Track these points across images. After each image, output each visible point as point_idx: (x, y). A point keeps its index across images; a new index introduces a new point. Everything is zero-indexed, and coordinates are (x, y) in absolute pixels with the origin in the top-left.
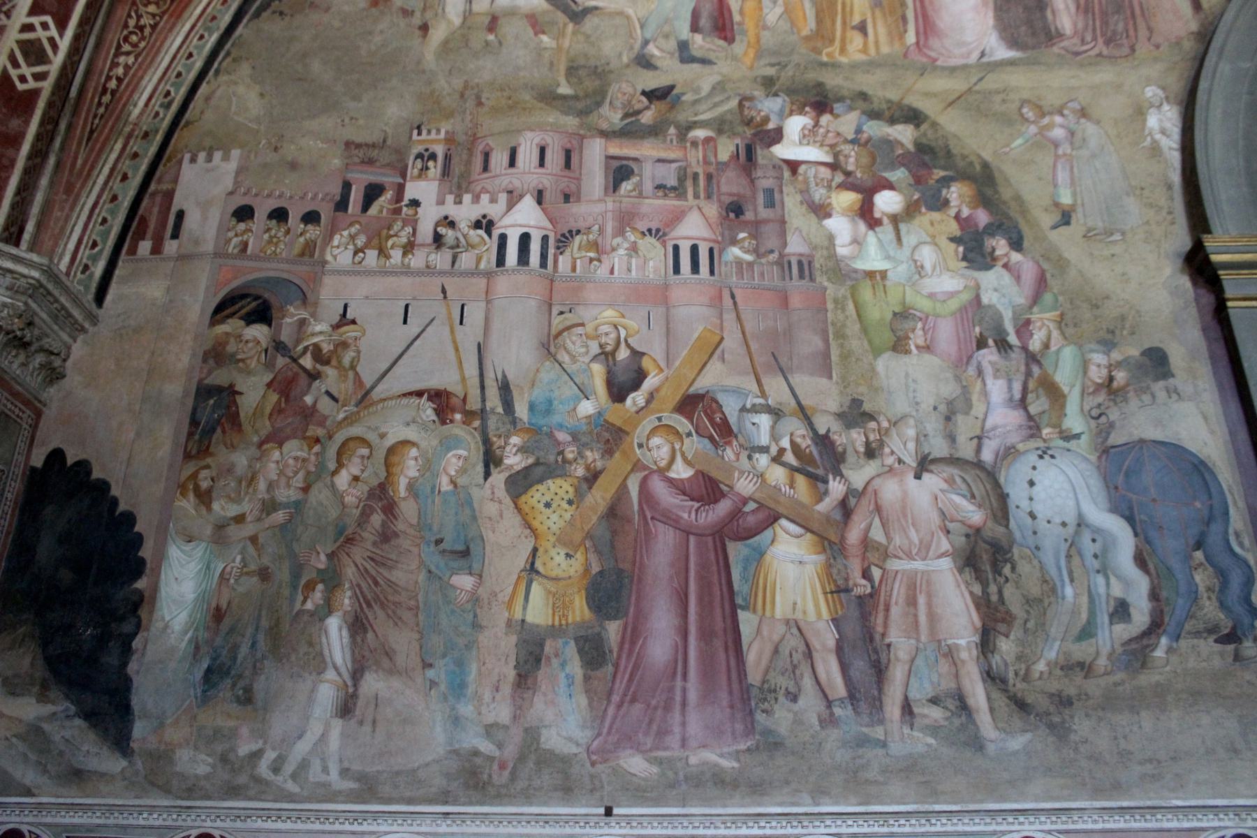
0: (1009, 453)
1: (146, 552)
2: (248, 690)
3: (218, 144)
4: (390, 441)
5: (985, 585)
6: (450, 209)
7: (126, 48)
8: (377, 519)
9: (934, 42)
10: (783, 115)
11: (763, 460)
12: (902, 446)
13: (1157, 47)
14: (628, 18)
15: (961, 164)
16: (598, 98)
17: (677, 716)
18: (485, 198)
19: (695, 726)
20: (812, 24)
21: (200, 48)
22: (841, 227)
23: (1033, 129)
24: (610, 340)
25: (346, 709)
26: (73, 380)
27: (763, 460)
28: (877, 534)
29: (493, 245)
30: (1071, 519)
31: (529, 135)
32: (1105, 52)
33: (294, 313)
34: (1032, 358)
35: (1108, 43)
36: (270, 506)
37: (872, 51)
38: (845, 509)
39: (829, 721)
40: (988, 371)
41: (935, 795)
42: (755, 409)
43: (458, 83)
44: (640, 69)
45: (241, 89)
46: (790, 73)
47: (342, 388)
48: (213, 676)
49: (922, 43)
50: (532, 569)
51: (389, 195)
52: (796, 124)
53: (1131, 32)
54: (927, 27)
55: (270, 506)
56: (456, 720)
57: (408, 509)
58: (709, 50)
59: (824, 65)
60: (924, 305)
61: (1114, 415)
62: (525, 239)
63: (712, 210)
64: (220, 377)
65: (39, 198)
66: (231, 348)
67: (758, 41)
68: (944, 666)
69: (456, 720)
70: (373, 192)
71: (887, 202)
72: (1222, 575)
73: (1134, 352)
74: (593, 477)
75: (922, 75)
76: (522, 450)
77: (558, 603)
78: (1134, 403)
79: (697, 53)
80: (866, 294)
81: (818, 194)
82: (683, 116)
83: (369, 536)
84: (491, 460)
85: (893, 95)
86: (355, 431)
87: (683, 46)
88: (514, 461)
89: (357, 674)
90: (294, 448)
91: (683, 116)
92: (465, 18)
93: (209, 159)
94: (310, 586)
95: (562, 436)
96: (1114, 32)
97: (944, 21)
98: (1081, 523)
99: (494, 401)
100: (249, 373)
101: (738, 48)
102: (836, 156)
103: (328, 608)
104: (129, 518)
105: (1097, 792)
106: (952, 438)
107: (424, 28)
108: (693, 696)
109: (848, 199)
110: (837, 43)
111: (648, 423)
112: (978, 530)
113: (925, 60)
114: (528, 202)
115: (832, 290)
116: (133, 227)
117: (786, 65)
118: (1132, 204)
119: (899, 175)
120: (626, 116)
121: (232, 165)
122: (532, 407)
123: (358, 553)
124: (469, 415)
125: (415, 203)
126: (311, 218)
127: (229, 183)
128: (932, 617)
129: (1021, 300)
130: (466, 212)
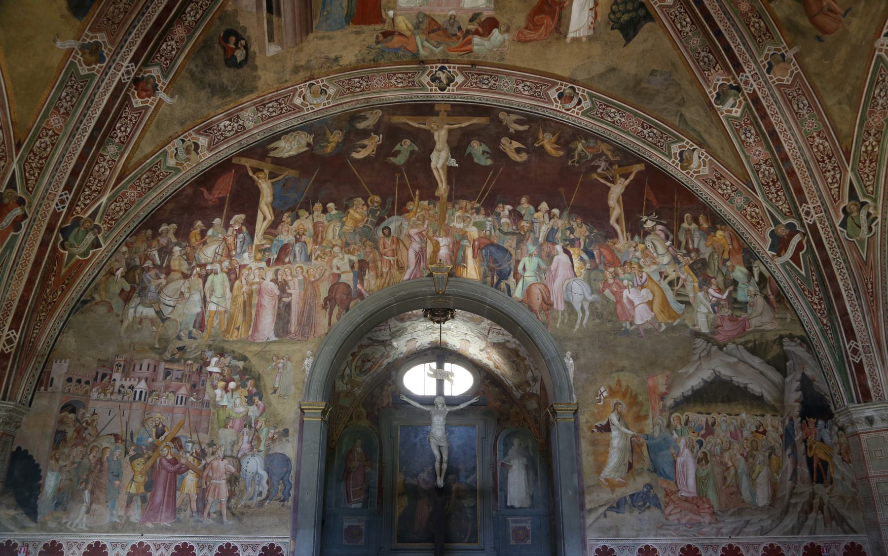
0: (245, 455)
1: (42, 474)
2: (66, 508)
3: (63, 357)
4: (104, 447)
5: (231, 486)
6: (123, 382)
7: (37, 327)
8: (99, 467)
9: (256, 335)
10: (212, 357)
11: (188, 455)
12: (220, 453)
14: (177, 322)
15: (253, 374)
16: (165, 349)
17: (159, 515)
18: (133, 379)
19: (163, 517)
21: (58, 327)
22: (218, 392)
23: (274, 364)
24: (158, 422)
25: (88, 512)
26: (23, 427)
27: (188, 455)
28: (210, 474)
29: (133, 394)
30: (254, 472)
31: (146, 360)
33: (82, 411)
34: (256, 430)
36: (73, 463)
38: (204, 468)
39: (192, 516)
40: (245, 433)
41: (211, 533)
42: (189, 442)
43: (129, 341)
45: (70, 339)
47: (93, 432)
48: (57, 505)
50: (133, 480)
51: (108, 377)
52: (214, 360)
54: (256, 329)
55: (73, 463)
56: (112, 515)
57: (106, 464)
59: (226, 341)
60: (234, 415)
61: (272, 446)
62: (141, 392)
63: (188, 386)
64: (62, 428)
65: (12, 378)
66: (65, 420)
68: (219, 505)
69: (112, 515)
70: (104, 376)
71: (232, 385)
72: (285, 486)
73: (281, 430)
74: (149, 458)
76: (134, 450)
77: (138, 488)
78: (277, 443)
79: (193, 336)
80: (221, 412)
81: (215, 382)
82: (186, 356)
83: (96, 471)
84: (126, 453)
85: (241, 352)
86: (95, 444)
87: (190, 332)
88: (132, 453)
89: (91, 504)
90: (80, 448)
91: (186, 356)
93: (60, 362)
94: (82, 483)
95: (143, 447)
97: (261, 327)
98: (257, 473)
99: (129, 438)
100: (69, 427)
101: (204, 334)
102: (222, 371)
103: (85, 488)
104: (38, 465)
105: (245, 534)
106: (232, 451)
107: (122, 321)
108: (164, 510)
109: (222, 384)
111: (164, 444)
112: (233, 474)
114: (143, 381)
115: (213, 410)
116: (40, 382)
118: (293, 387)
119: (237, 377)
120: (172, 355)
121: (66, 365)
122: (137, 439)
123: (94, 475)
124: (123, 441)
125: (115, 380)
126: (87, 383)
127: (66, 370)
128: (218, 494)
129: (258, 415)
130: (127, 384)
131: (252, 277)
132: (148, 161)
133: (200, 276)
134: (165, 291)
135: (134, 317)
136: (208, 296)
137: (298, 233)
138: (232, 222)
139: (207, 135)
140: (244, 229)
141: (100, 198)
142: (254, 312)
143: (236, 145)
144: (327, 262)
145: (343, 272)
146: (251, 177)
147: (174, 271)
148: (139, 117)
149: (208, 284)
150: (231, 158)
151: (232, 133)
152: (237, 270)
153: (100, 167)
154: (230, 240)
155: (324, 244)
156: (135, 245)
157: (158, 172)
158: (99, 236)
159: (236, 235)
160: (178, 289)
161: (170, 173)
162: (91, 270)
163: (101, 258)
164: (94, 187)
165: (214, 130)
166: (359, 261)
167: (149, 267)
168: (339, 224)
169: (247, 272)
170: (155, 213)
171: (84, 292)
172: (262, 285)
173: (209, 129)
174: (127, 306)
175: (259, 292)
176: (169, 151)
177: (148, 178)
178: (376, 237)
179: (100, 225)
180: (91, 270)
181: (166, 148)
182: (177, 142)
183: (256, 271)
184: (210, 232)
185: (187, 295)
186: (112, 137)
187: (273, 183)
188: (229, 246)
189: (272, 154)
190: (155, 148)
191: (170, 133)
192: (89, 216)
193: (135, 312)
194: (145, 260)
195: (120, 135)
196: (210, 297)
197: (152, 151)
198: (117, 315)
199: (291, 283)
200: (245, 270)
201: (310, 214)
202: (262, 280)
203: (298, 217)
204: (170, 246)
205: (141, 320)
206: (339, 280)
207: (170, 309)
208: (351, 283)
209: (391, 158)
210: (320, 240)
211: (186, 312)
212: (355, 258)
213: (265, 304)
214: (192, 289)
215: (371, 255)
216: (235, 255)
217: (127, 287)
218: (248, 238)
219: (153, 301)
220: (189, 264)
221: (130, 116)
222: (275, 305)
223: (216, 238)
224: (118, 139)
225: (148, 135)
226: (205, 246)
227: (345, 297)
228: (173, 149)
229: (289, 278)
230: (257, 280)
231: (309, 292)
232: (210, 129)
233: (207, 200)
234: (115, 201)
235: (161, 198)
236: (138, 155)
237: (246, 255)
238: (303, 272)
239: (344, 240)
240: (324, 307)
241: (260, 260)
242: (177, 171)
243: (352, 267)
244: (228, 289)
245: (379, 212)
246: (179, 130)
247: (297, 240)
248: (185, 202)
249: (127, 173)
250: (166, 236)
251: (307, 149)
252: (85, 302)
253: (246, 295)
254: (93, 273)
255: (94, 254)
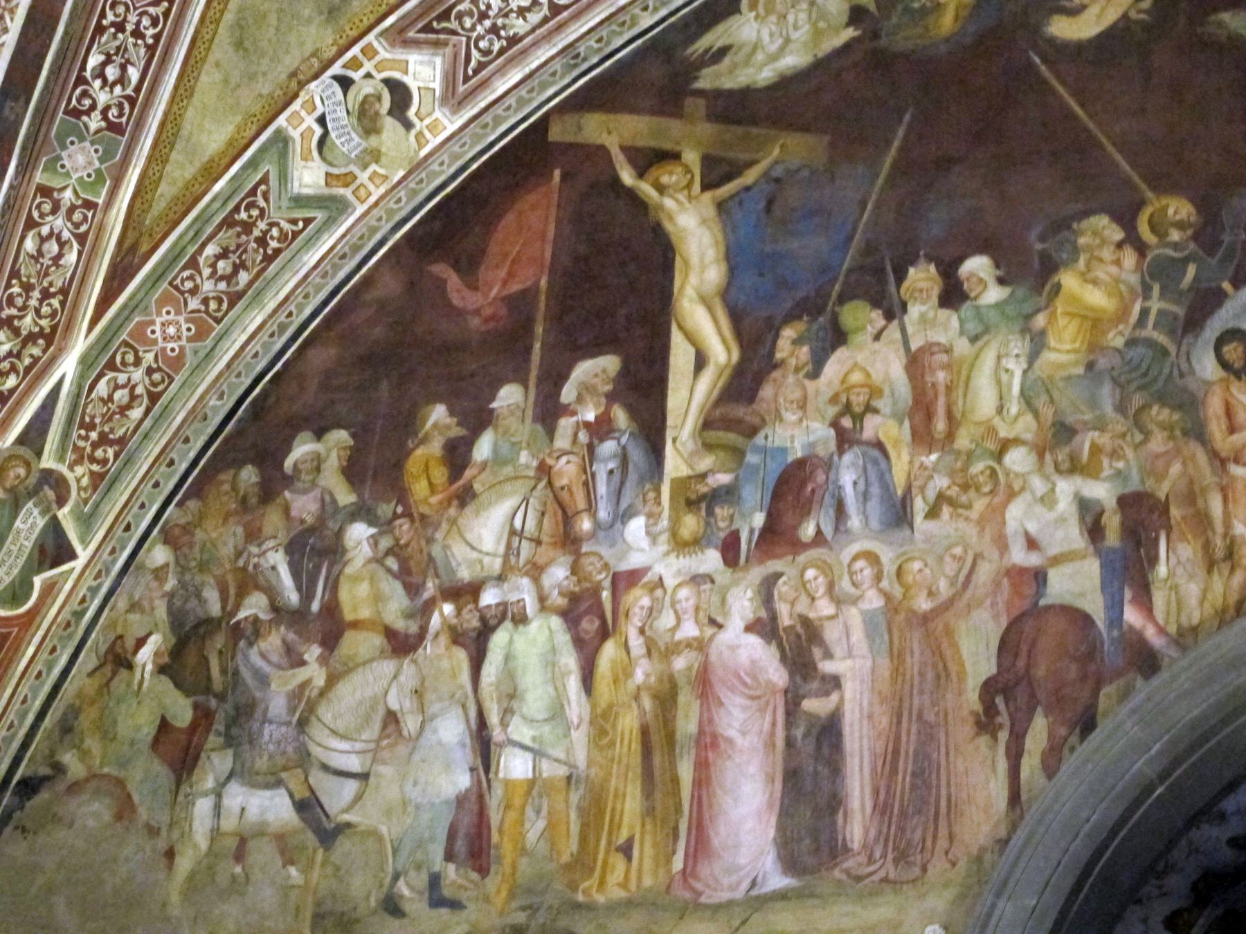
9: (704, 870)
13: (954, 864)
14: (380, 838)
20: (574, 846)
32: (892, 876)
35: (896, 861)
37: (633, 886)
44: (387, 917)
46: (541, 921)
49: (688, 871)
53: (929, 843)
54: (700, 846)
58: (461, 887)
59: (578, 906)
67: (513, 874)
75: (681, 918)
79: (447, 892)
87: (435, 881)
92: (212, 840)
96: (909, 843)
97: (719, 835)
101: (493, 883)
107: (170, 854)
110: (597, 874)
113: (688, 895)
117: (538, 909)
131: (666, 620)
132: (218, 187)
133: (456, 636)
134: (325, 712)
135: (216, 833)
136: (493, 719)
137: (847, 409)
138: (568, 394)
139: (437, 44)
140: (620, 416)
141: (53, 360)
142: (686, 771)
143: (557, 65)
144: (981, 523)
145: (1056, 560)
146: (632, 196)
147: (355, 625)
148: (166, 14)
149: (491, 670)
150: (542, 126)
151: (534, 18)
152: (606, 595)
153: (43, 240)
154: (567, 470)
155: (963, 441)
156: (199, 535)
157: (262, 225)
158: (64, 514)
159: (591, 448)
160: (374, 702)
161: (307, 221)
162: (44, 655)
163: (74, 605)
164: (28, 320)
165: (460, 16)
166: (1125, 502)
167: (256, 620)
168: (1018, 346)
169: (646, 601)
170: (265, 394)
171: (25, 746)
172: (713, 657)
173: (440, 18)
174: (185, 788)
175: (703, 681)
176: (295, 134)
177: (224, 254)
178: (1191, 384)
179: (63, 469)
180: (44, 655)
181: (281, 121)
182: (321, 90)
183: (683, 593)
184: (483, 448)
185: (411, 724)
186: (76, 113)
187: (721, 206)
188: (565, 495)
189: (707, 80)
190: (239, 129)
191: (291, 61)
192: (21, 440)
193: (218, 807)
194: (242, 593)
195: (103, 98)
196: (504, 724)
197: (230, 143)
198: (153, 832)
199: (832, 633)
200: (636, 592)
201: (889, 316)
202: (709, 631)
203: (838, 337)
204: (333, 525)
205: (243, 841)
206: (1039, 593)
207: (351, 787)
208: (1095, 606)
209: (1226, 16)
210: (940, 425)
211: (414, 793)
212: (1102, 491)
213: (732, 733)
214: (430, 696)
215: (1176, 469)
216: (593, 535)
217: (182, 711)
218: (637, 455)
219: (280, 761)
220: (412, 589)
221: (132, 18)
222: (772, 734)
223: (508, 470)
224: (96, 115)
225: (208, 79)
226: (468, 510)
227: (1073, 671)
228: (310, 121)
229: (825, 608)
230: (689, 630)
231: (913, 663)
232: (445, 16)
233: (460, 313)
234: (111, 366)
235: (282, 328)
236: (180, 170)
237: (636, 527)
238: (878, 577)
239: (1048, 413)
240: (986, 723)
241: (697, 543)
242: (334, 207)
243: (1095, 531)
244: (573, 684)
245: (1191, 271)
246: (320, 37)
247: (844, 440)
248: (378, 332)
249: (144, 248)
250: (314, 484)
251: (850, 33)
252: (29, 787)
253: (647, 703)
254: (50, 668)
255: (50, 589)
